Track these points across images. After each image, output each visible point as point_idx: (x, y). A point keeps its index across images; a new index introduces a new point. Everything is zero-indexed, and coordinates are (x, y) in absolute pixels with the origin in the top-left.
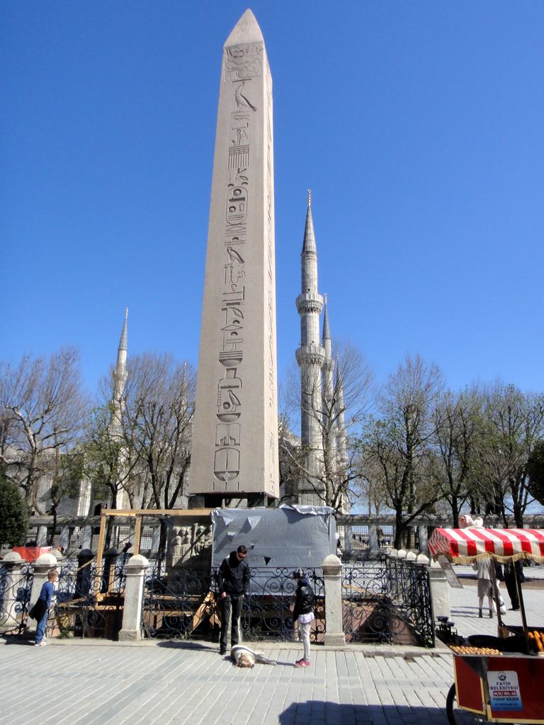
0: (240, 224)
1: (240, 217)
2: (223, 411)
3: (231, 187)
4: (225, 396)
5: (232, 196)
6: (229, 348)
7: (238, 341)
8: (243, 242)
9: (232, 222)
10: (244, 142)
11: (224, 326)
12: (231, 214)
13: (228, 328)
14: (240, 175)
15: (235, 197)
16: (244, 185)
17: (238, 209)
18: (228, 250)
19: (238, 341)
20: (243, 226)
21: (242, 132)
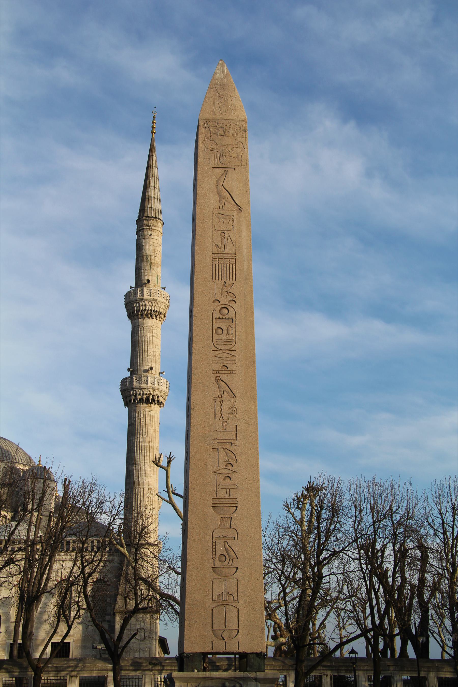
1: (228, 342)
2: (218, 564)
3: (217, 303)
4: (220, 550)
5: (217, 315)
6: (222, 494)
7: (233, 487)
8: (232, 373)
9: (220, 347)
10: (230, 249)
11: (216, 468)
12: (218, 337)
13: (220, 472)
14: (225, 290)
15: (221, 317)
16: (232, 304)
18: (216, 380)
19: (233, 487)
20: (233, 353)
21: (227, 235)
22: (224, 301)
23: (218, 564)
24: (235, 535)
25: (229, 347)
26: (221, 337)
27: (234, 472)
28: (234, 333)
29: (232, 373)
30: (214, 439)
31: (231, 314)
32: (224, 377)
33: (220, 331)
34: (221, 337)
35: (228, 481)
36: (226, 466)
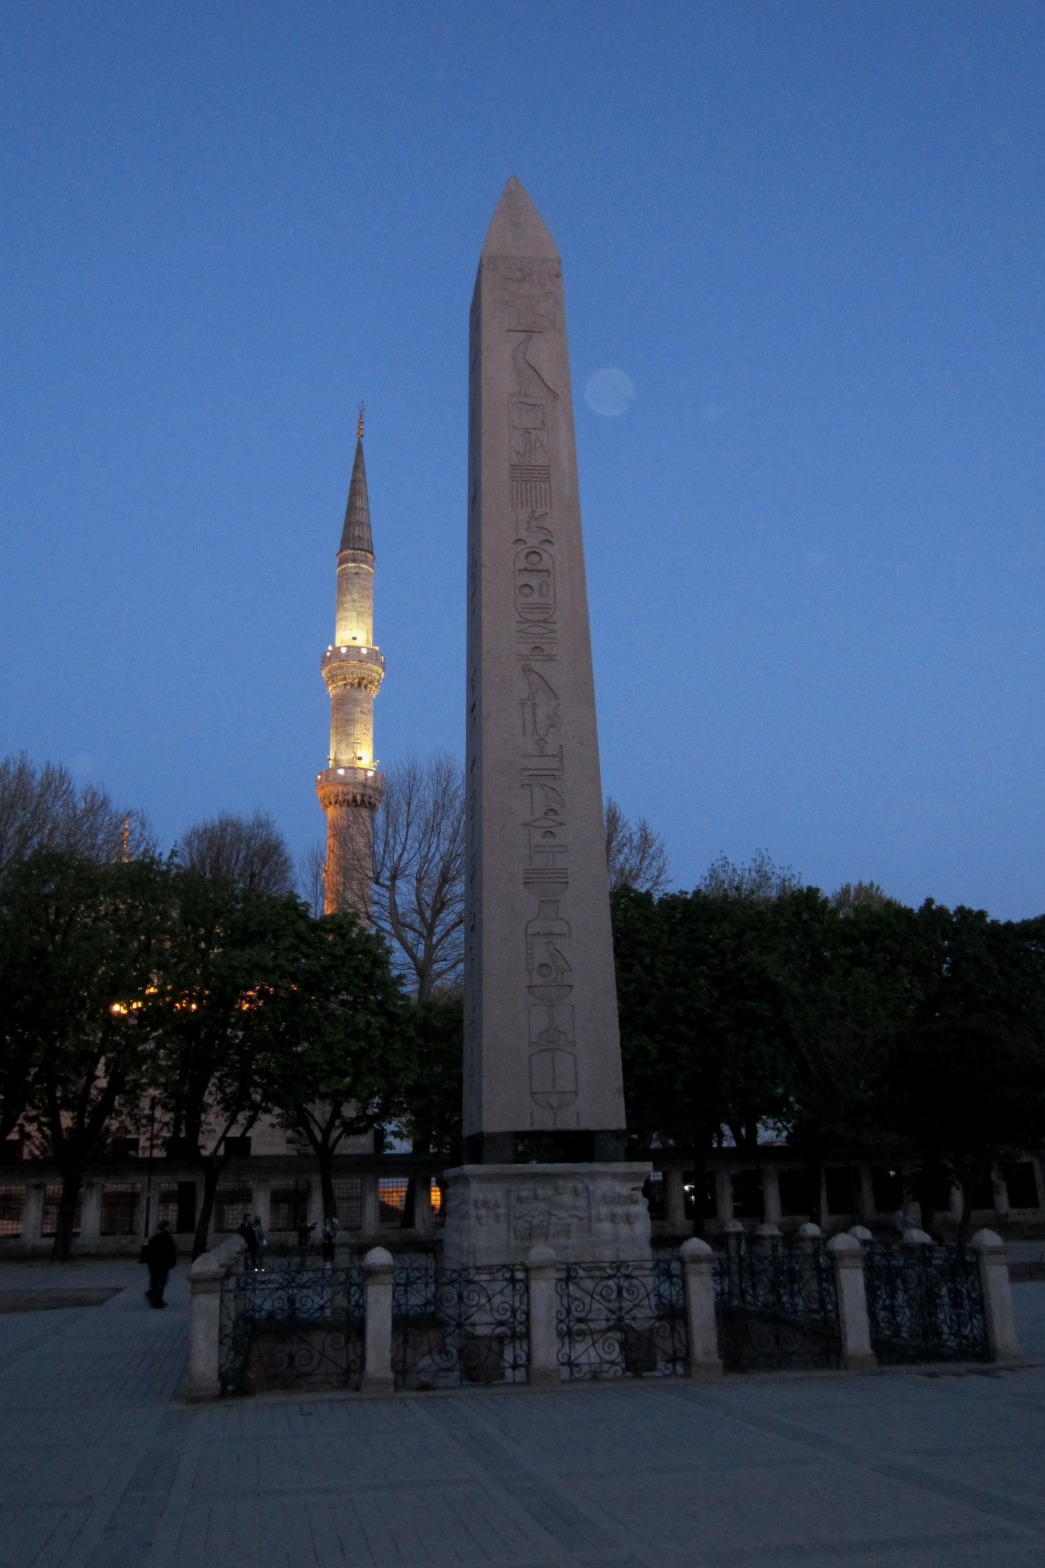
0: (545, 621)
2: (538, 980)
3: (521, 546)
5: (521, 564)
8: (550, 658)
9: (528, 616)
13: (537, 824)
15: (529, 567)
17: (536, 593)
20: (552, 627)
22: (533, 541)
23: (538, 980)
24: (565, 930)
25: (545, 616)
26: (530, 600)
27: (561, 824)
28: (551, 593)
29: (550, 658)
30: (524, 770)
31: (546, 563)
32: (537, 666)
33: (527, 590)
34: (530, 600)
35: (551, 841)
36: (546, 813)
